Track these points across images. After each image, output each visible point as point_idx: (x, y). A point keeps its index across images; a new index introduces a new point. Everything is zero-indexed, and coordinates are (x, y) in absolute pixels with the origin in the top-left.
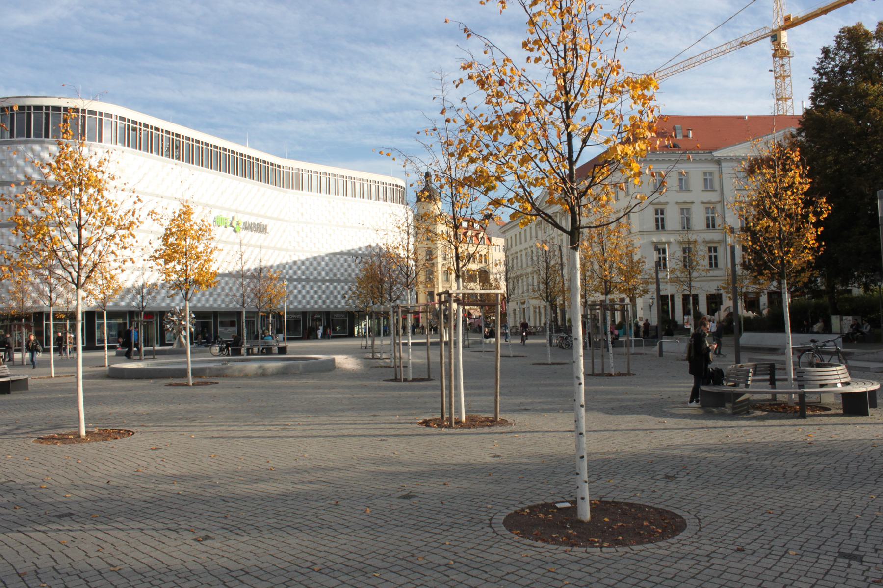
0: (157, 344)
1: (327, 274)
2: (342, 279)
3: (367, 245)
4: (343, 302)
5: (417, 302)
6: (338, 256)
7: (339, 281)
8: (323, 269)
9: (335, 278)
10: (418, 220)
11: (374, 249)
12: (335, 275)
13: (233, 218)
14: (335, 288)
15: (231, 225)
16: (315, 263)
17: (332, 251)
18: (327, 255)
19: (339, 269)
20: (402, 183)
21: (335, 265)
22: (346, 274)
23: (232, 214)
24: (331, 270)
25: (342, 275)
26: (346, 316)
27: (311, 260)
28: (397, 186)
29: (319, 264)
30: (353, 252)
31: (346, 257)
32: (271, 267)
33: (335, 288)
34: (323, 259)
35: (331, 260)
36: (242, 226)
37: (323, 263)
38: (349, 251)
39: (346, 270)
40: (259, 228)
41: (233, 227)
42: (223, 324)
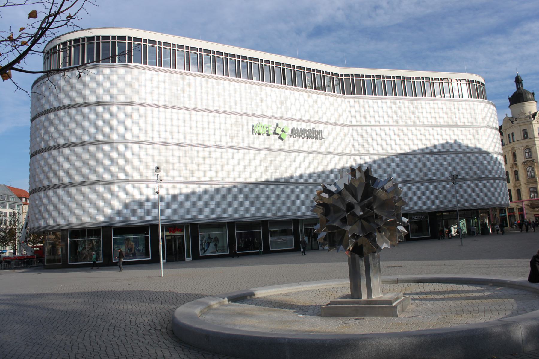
0: (189, 257)
1: (399, 176)
2: (417, 179)
3: (443, 142)
4: (420, 204)
5: (511, 200)
6: (411, 156)
7: (413, 182)
8: (394, 170)
9: (408, 179)
10: (512, 122)
11: (451, 145)
12: (408, 176)
13: (277, 125)
14: (410, 189)
15: (275, 133)
16: (384, 166)
17: (402, 152)
18: (397, 156)
19: (412, 170)
20: (482, 80)
21: (407, 166)
22: (421, 174)
23: (276, 121)
24: (403, 171)
25: (417, 175)
26: (426, 217)
27: (380, 162)
28: (473, 81)
29: (389, 166)
30: (428, 151)
31: (419, 156)
32: (332, 171)
33: (410, 189)
34: (393, 161)
35: (402, 160)
36: (289, 132)
37: (393, 165)
38: (422, 150)
39: (421, 170)
40: (317, 135)
41: (277, 134)
42: (273, 233)
